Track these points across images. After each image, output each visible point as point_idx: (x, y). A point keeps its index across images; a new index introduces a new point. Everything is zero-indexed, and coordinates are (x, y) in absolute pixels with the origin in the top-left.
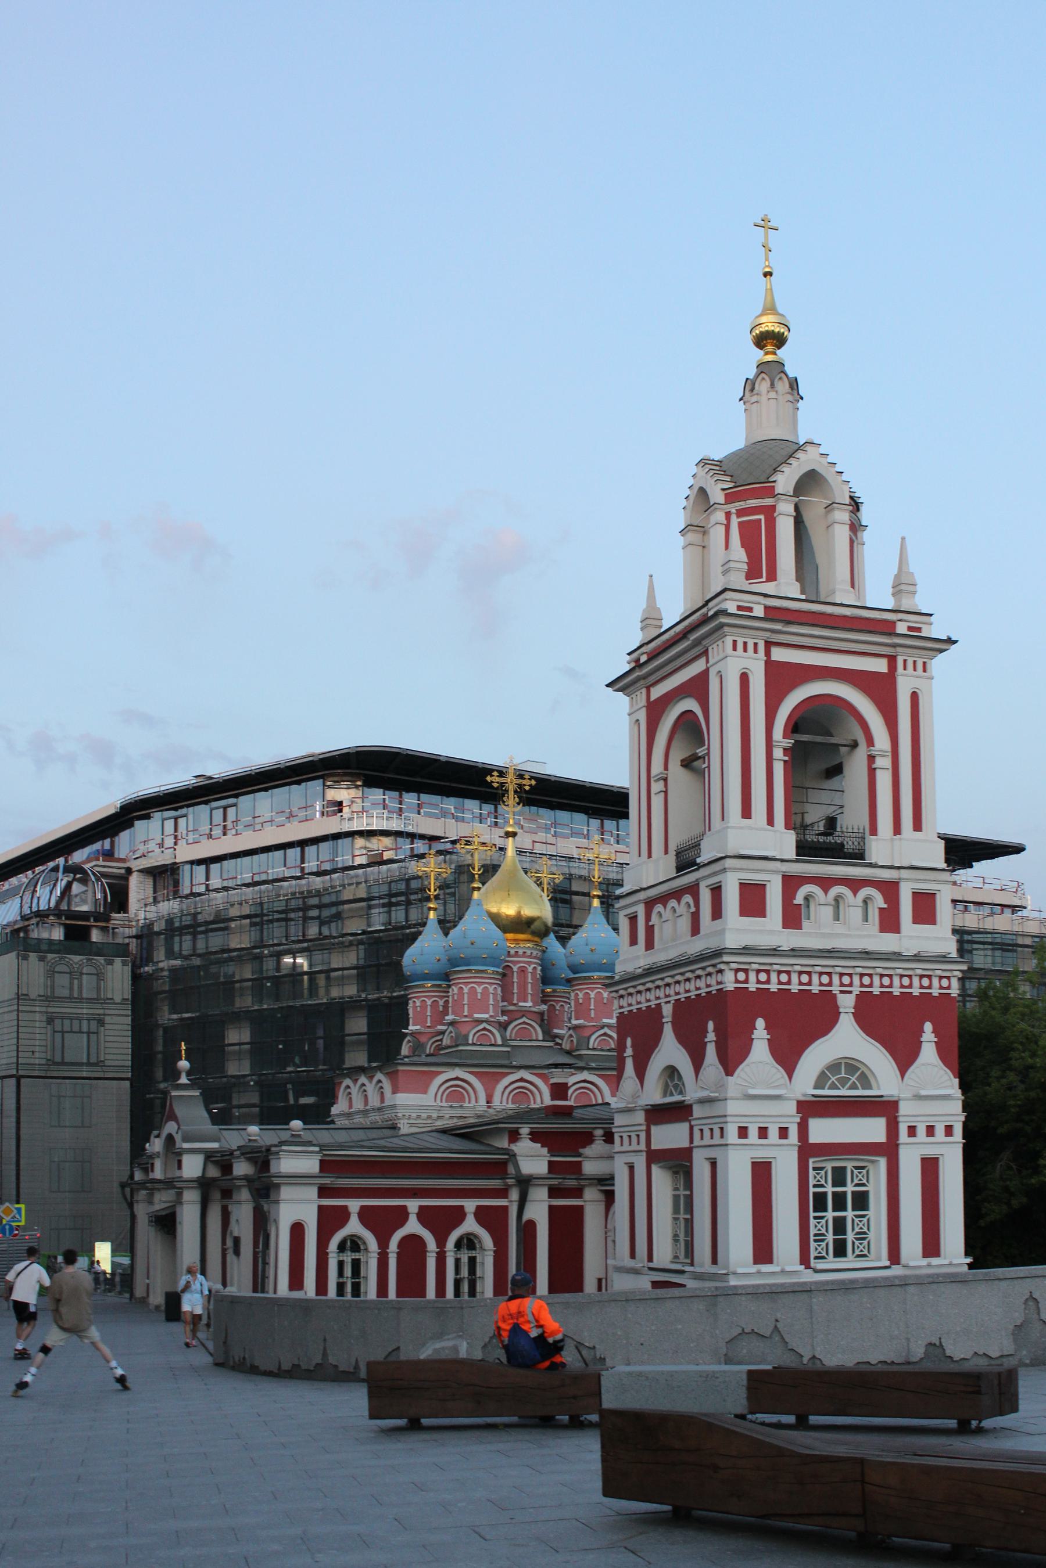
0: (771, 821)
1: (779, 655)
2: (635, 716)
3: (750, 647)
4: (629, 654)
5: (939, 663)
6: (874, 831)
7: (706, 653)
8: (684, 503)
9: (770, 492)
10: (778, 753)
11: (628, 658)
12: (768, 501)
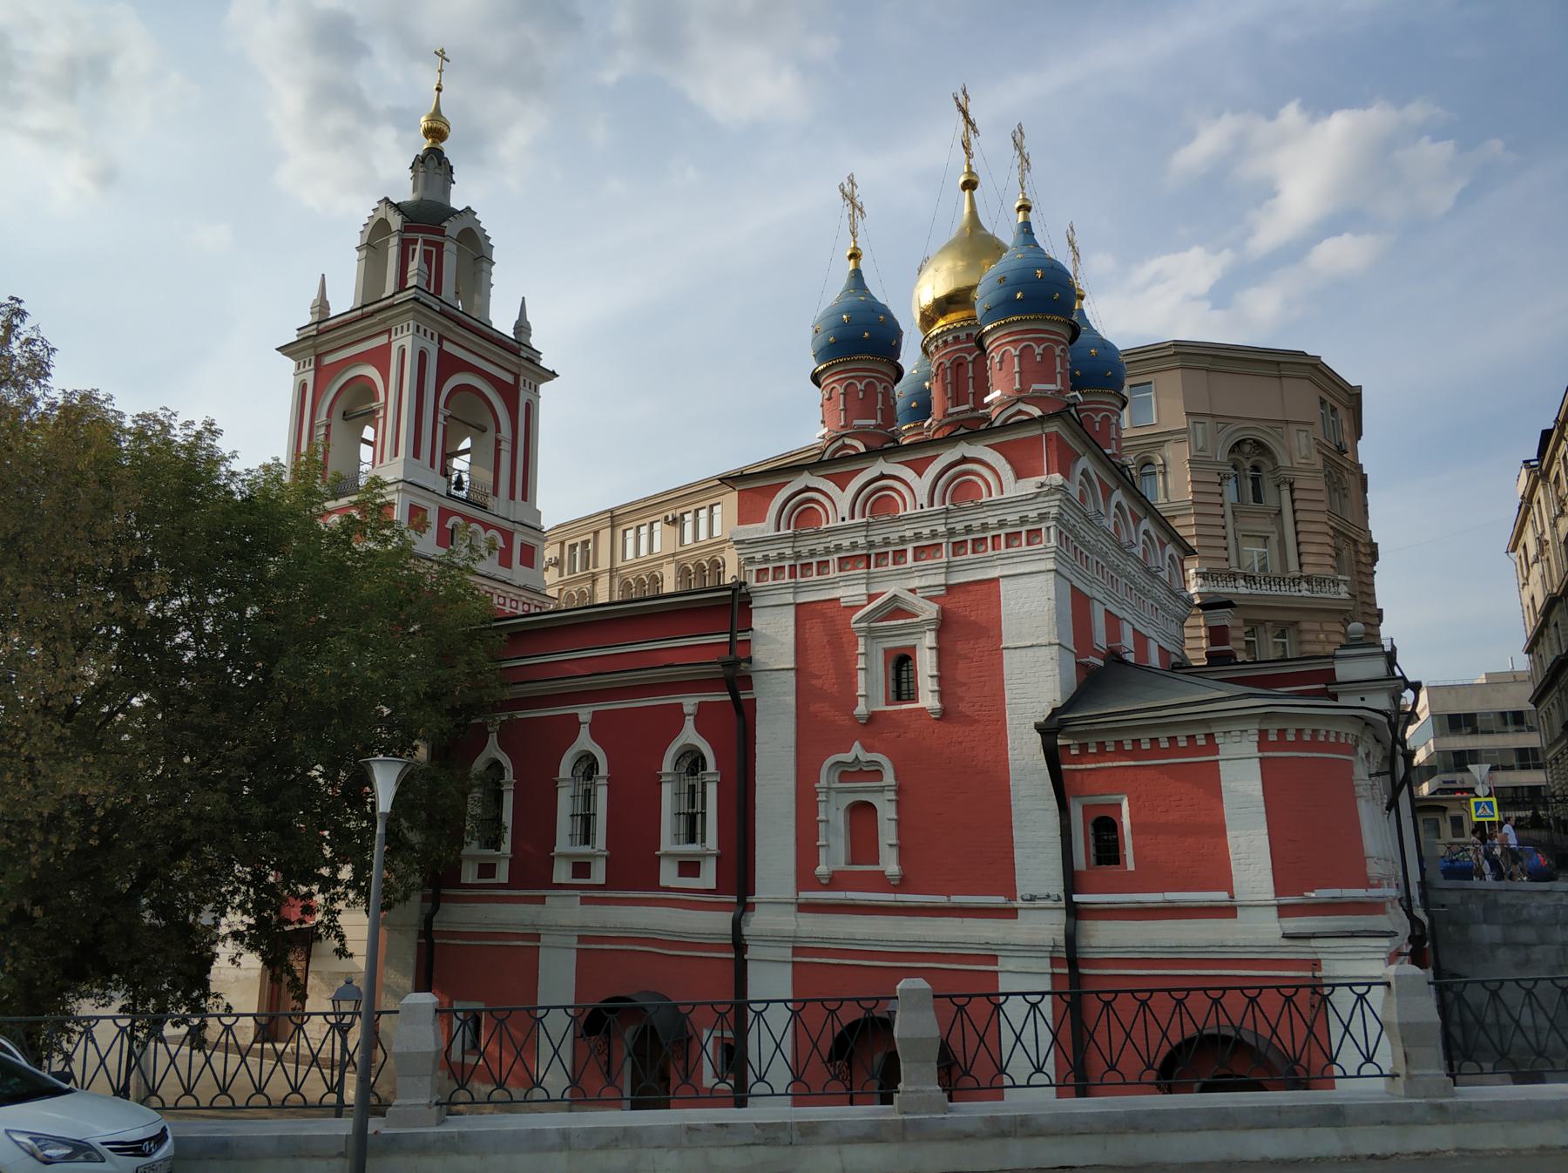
0: (432, 465)
1: (447, 346)
2: (302, 377)
3: (429, 334)
4: (298, 330)
5: (544, 388)
6: (496, 493)
7: (389, 331)
8: (362, 228)
9: (442, 233)
10: (441, 418)
11: (297, 332)
12: (438, 238)
